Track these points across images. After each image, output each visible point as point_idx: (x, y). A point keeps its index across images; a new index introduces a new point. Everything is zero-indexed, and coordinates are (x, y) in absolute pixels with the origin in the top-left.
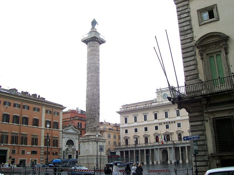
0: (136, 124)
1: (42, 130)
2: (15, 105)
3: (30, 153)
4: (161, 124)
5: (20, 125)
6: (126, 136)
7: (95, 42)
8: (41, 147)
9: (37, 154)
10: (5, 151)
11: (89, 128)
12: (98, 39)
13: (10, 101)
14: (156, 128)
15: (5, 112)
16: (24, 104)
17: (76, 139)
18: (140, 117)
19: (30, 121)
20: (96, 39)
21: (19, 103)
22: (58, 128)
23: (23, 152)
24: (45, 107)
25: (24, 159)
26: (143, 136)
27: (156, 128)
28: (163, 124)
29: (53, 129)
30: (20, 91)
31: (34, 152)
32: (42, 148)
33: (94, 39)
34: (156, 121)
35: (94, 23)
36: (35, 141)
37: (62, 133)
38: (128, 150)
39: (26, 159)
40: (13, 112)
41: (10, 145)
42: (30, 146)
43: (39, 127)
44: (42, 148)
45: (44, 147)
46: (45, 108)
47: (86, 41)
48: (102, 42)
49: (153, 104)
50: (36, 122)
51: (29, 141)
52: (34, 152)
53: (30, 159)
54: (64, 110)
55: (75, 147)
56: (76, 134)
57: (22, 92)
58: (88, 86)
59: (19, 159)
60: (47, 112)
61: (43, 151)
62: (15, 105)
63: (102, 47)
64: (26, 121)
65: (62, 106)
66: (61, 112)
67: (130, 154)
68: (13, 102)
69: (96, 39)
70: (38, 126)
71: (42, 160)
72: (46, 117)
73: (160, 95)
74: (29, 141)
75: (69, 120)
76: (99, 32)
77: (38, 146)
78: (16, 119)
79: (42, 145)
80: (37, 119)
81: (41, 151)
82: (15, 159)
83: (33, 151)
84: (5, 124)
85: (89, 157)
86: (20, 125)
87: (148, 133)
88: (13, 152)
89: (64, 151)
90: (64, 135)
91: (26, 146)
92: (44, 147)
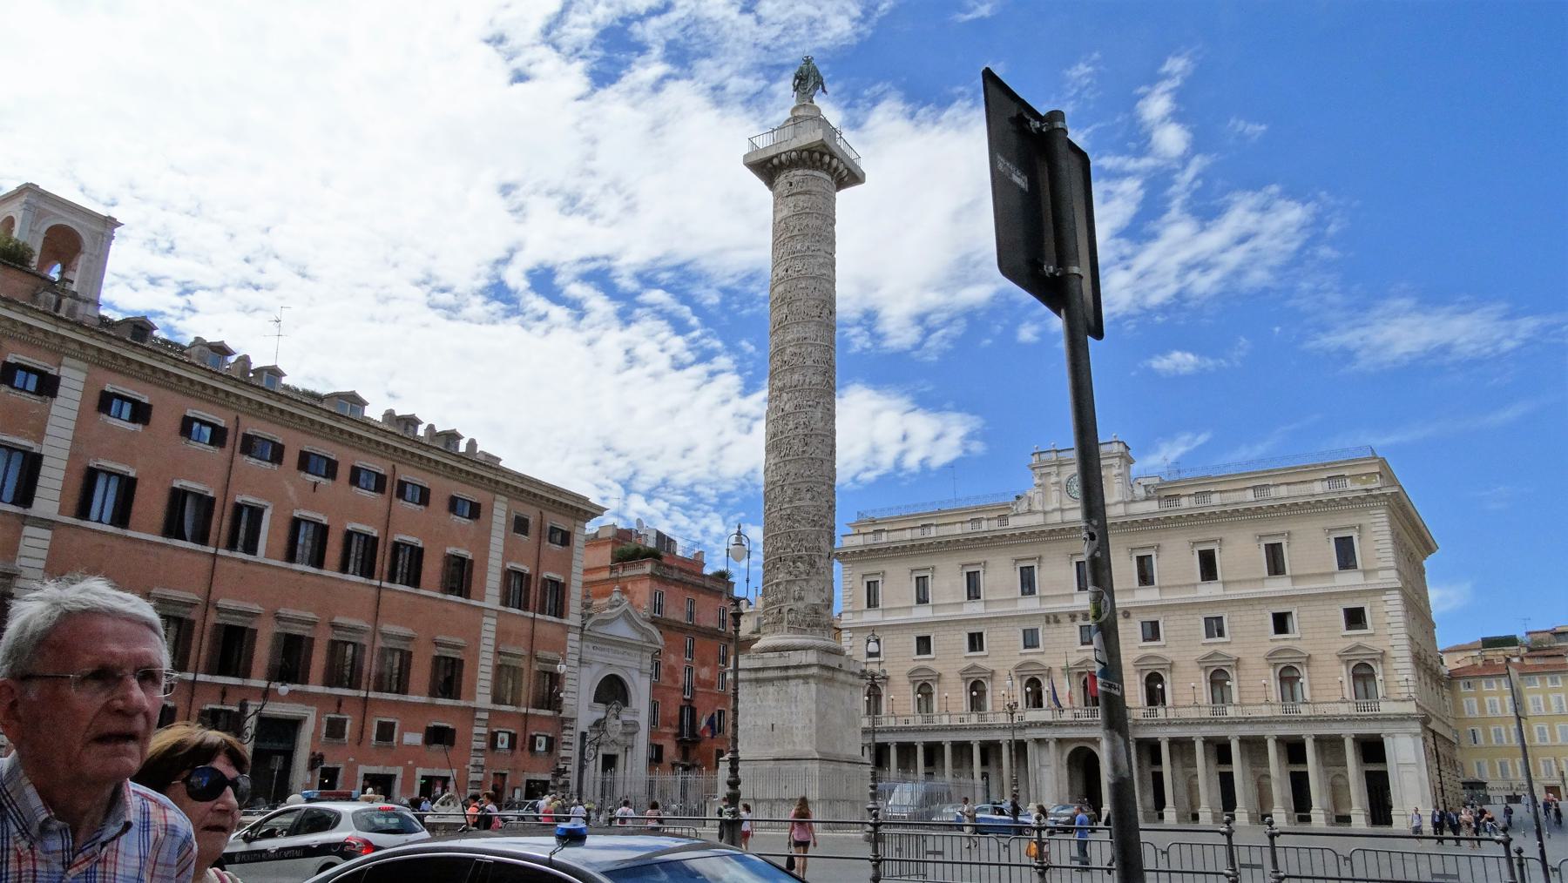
0: (923, 613)
1: (485, 620)
2: (355, 476)
3: (415, 738)
4: (1053, 619)
5: (380, 587)
6: (974, 667)
7: (816, 173)
8: (475, 710)
9: (452, 743)
10: (294, 725)
11: (785, 610)
12: (832, 156)
14: (1031, 640)
16: (406, 474)
17: (641, 672)
18: (948, 581)
19: (432, 568)
20: (827, 159)
22: (560, 610)
23: (386, 732)
26: (911, 674)
27: (1031, 640)
28: (1066, 620)
29: (538, 616)
30: (374, 413)
31: (439, 736)
32: (479, 715)
33: (817, 155)
34: (1030, 605)
37: (577, 637)
39: (399, 771)
40: (351, 511)
42: (423, 699)
43: (473, 602)
44: (479, 715)
45: (492, 707)
47: (767, 168)
48: (852, 177)
49: (1013, 522)
50: (460, 576)
51: (421, 673)
52: (439, 736)
53: (420, 772)
54: (592, 527)
55: (636, 713)
56: (642, 649)
57: (389, 415)
58: (781, 390)
61: (484, 730)
62: (355, 476)
63: (845, 199)
65: (585, 500)
66: (577, 530)
69: (827, 159)
70: (468, 597)
71: (479, 777)
73: (1053, 479)
74: (421, 673)
75: (605, 575)
77: (462, 703)
78: (363, 554)
79: (483, 700)
80: (463, 560)
81: (476, 730)
82: (340, 776)
84: (303, 573)
85: (784, 766)
87: (983, 661)
88: (335, 729)
89: (583, 735)
90: (589, 652)
91: (402, 698)
92: (490, 711)
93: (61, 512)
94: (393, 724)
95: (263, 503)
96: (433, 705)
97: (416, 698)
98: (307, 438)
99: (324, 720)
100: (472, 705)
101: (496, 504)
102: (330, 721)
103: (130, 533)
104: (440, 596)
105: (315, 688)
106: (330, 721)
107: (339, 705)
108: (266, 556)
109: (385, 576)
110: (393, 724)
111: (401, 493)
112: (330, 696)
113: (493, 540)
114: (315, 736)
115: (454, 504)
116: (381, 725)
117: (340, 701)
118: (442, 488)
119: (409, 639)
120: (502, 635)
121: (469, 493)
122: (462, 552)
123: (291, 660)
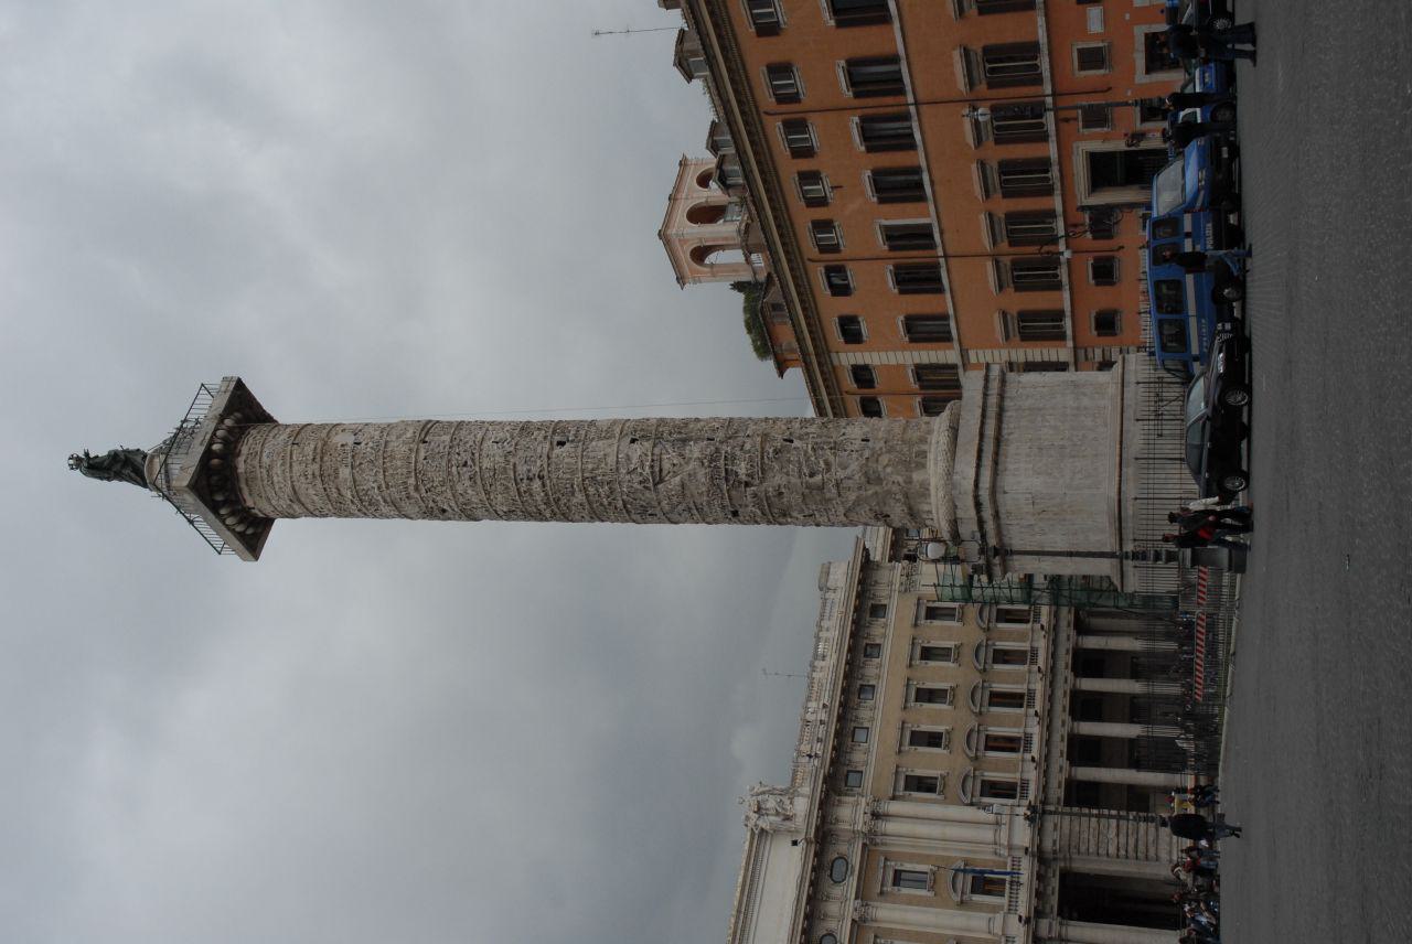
13: (775, 128)
15: (863, 193)
16: (766, 99)
23: (1092, 59)
25: (1143, 48)
35: (118, 466)
38: (1065, 646)
41: (1066, 295)
42: (1041, 21)
59: (1141, 77)
64: (874, 79)
67: (1112, 720)
68: (789, 169)
76: (136, 448)
78: (884, 135)
83: (1094, 278)
84: (932, 183)
86: (946, 256)
88: (1096, 117)
93: (953, 348)
94: (1080, 51)
95: (878, 228)
97: (1052, 150)
98: (742, 38)
99: (1086, 131)
103: (951, 312)
104: (897, 25)
105: (1052, 150)
108: (929, 215)
109: (899, 99)
110: (1080, 51)
114: (1105, 139)
116: (1082, 68)
119: (967, 53)
123: (1022, 177)
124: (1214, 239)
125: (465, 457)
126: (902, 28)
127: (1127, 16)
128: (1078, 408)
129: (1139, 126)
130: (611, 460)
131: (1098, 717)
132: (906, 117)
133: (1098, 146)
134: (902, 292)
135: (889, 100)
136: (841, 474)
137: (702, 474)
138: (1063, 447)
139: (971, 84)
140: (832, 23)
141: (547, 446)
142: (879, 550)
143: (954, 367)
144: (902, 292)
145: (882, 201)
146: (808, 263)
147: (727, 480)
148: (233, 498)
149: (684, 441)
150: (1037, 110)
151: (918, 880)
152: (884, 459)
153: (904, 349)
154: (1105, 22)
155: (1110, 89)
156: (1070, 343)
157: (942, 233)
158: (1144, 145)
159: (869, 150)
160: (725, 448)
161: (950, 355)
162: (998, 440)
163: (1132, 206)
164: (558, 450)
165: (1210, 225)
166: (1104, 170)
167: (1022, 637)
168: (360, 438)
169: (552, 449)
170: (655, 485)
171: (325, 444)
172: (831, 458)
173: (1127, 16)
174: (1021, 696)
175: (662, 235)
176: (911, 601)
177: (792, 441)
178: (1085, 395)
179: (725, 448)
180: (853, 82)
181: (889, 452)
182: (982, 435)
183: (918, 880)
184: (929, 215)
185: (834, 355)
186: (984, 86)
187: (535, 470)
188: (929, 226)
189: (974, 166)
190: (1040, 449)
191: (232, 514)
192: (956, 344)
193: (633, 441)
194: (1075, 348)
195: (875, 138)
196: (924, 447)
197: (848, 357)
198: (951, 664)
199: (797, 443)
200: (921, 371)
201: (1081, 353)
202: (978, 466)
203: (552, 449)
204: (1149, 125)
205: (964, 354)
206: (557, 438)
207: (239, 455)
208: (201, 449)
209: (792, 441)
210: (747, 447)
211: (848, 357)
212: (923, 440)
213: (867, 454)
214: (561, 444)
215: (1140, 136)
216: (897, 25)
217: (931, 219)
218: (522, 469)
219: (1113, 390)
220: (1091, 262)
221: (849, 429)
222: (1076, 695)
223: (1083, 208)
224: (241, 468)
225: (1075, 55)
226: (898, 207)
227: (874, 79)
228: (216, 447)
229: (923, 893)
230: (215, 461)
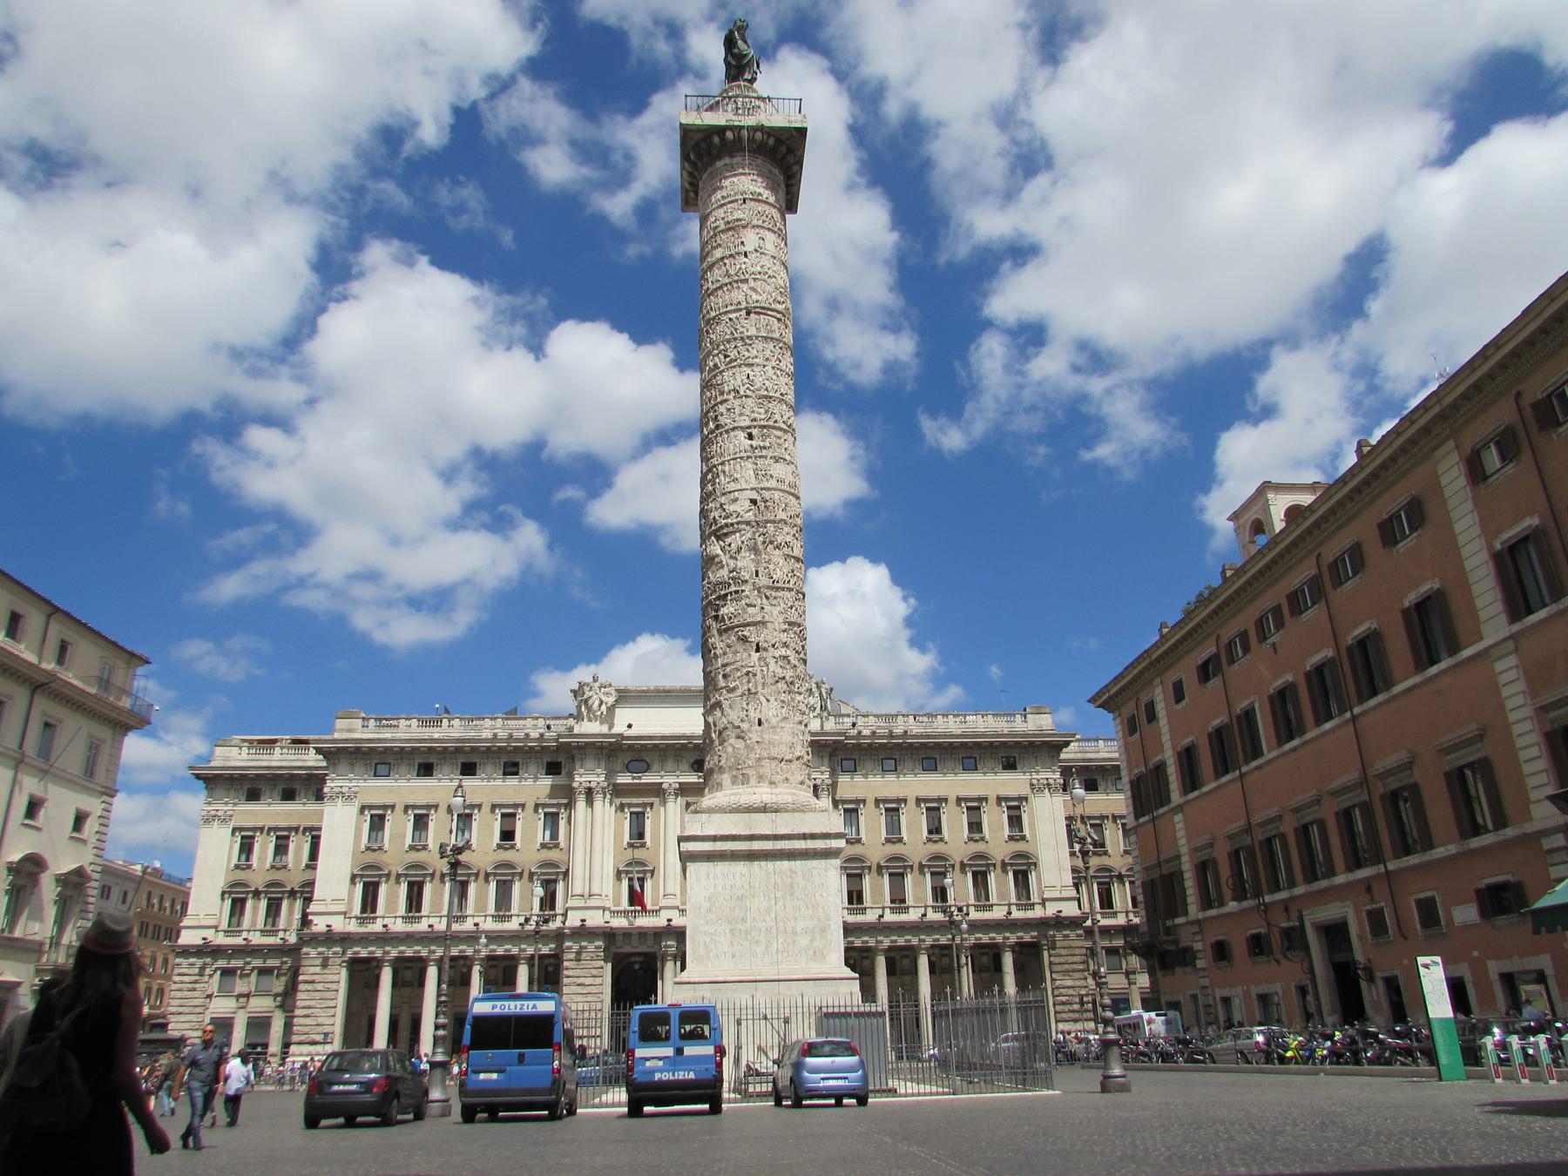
1: (1499, 666)
5: (1354, 718)
15: (1275, 677)
21: (1306, 571)
23: (1428, 912)
24: (1451, 444)
32: (1548, 843)
36: (1475, 789)
42: (1452, 849)
44: (1548, 843)
46: (1455, 457)
53: (1494, 968)
60: (1476, 471)
64: (1366, 666)
72: (1488, 527)
74: (1440, 811)
78: (1325, 689)
84: (1294, 749)
88: (1377, 922)
96: (1472, 852)
99: (1364, 915)
100: (1529, 828)
101: (1441, 468)
102: (1370, 914)
103: (1205, 789)
104: (1417, 679)
105: (1340, 879)
106: (1370, 914)
107: (1369, 890)
109: (1354, 700)
111: (1338, 582)
112: (1360, 881)
113: (1458, 527)
114: (1361, 937)
115: (1389, 533)
116: (1420, 903)
117: (1368, 886)
118: (1363, 529)
120: (1535, 677)
121: (1391, 502)
122: (1425, 588)
124: (668, 1081)
125: (733, 354)
126: (1415, 686)
127: (1476, 954)
128: (794, 933)
129: (1379, 975)
130: (732, 486)
131: (891, 972)
132: (1342, 711)
133: (1353, 930)
134: (1210, 735)
135: (1352, 689)
136: (725, 704)
137: (724, 573)
138: (744, 920)
139: (1380, 777)
140: (1407, 604)
141: (747, 423)
142: (1071, 756)
143: (1169, 801)
144: (1210, 735)
145: (1271, 698)
146: (1213, 639)
147: (719, 598)
148: (700, 165)
149: (754, 549)
150: (1379, 859)
151: (638, 834)
152: (739, 744)
153: (1174, 747)
154: (1466, 927)
155: (1405, 938)
156: (1201, 916)
157: (1259, 768)
158: (1363, 984)
159: (1308, 675)
160: (747, 588)
161: (1176, 796)
162: (751, 856)
163: (1312, 971)
164: (742, 435)
165: (692, 1075)
166: (1335, 934)
167: (1002, 895)
168: (752, 256)
169: (742, 428)
170: (714, 533)
171: (744, 227)
172: (739, 692)
173: (1476, 954)
174: (860, 900)
175: (1266, 487)
176: (1024, 790)
177: (758, 650)
178: (812, 940)
179: (747, 588)
180: (1362, 643)
181: (747, 747)
182: (752, 838)
183: (638, 834)
184: (1270, 751)
185: (1158, 680)
186: (1381, 791)
187: (722, 420)
188: (1262, 754)
189: (1314, 792)
190: (741, 898)
191: (691, 174)
192: (1182, 800)
193: (754, 502)
194: (1198, 922)
195: (1319, 676)
196: (753, 781)
197: (1160, 696)
198: (884, 835)
199: (755, 656)
200: (1160, 768)
201: (1196, 929)
202: (715, 838)
203: (742, 428)
204: (1381, 984)
205: (1179, 808)
206: (755, 432)
207: (732, 156)
208: (723, 123)
209: (758, 650)
210: (751, 610)
211: (1160, 696)
212: (761, 778)
213: (745, 726)
214: (750, 437)
215: (1371, 979)
216: (1417, 679)
217: (1269, 755)
218: (722, 409)
219: (816, 970)
220: (1262, 930)
221: (773, 703)
222: (911, 952)
223: (1301, 918)
224: (719, 164)
225: (1429, 894)
226: (1270, 718)
227: (1366, 666)
228: (729, 135)
229: (627, 838)
230: (716, 140)
